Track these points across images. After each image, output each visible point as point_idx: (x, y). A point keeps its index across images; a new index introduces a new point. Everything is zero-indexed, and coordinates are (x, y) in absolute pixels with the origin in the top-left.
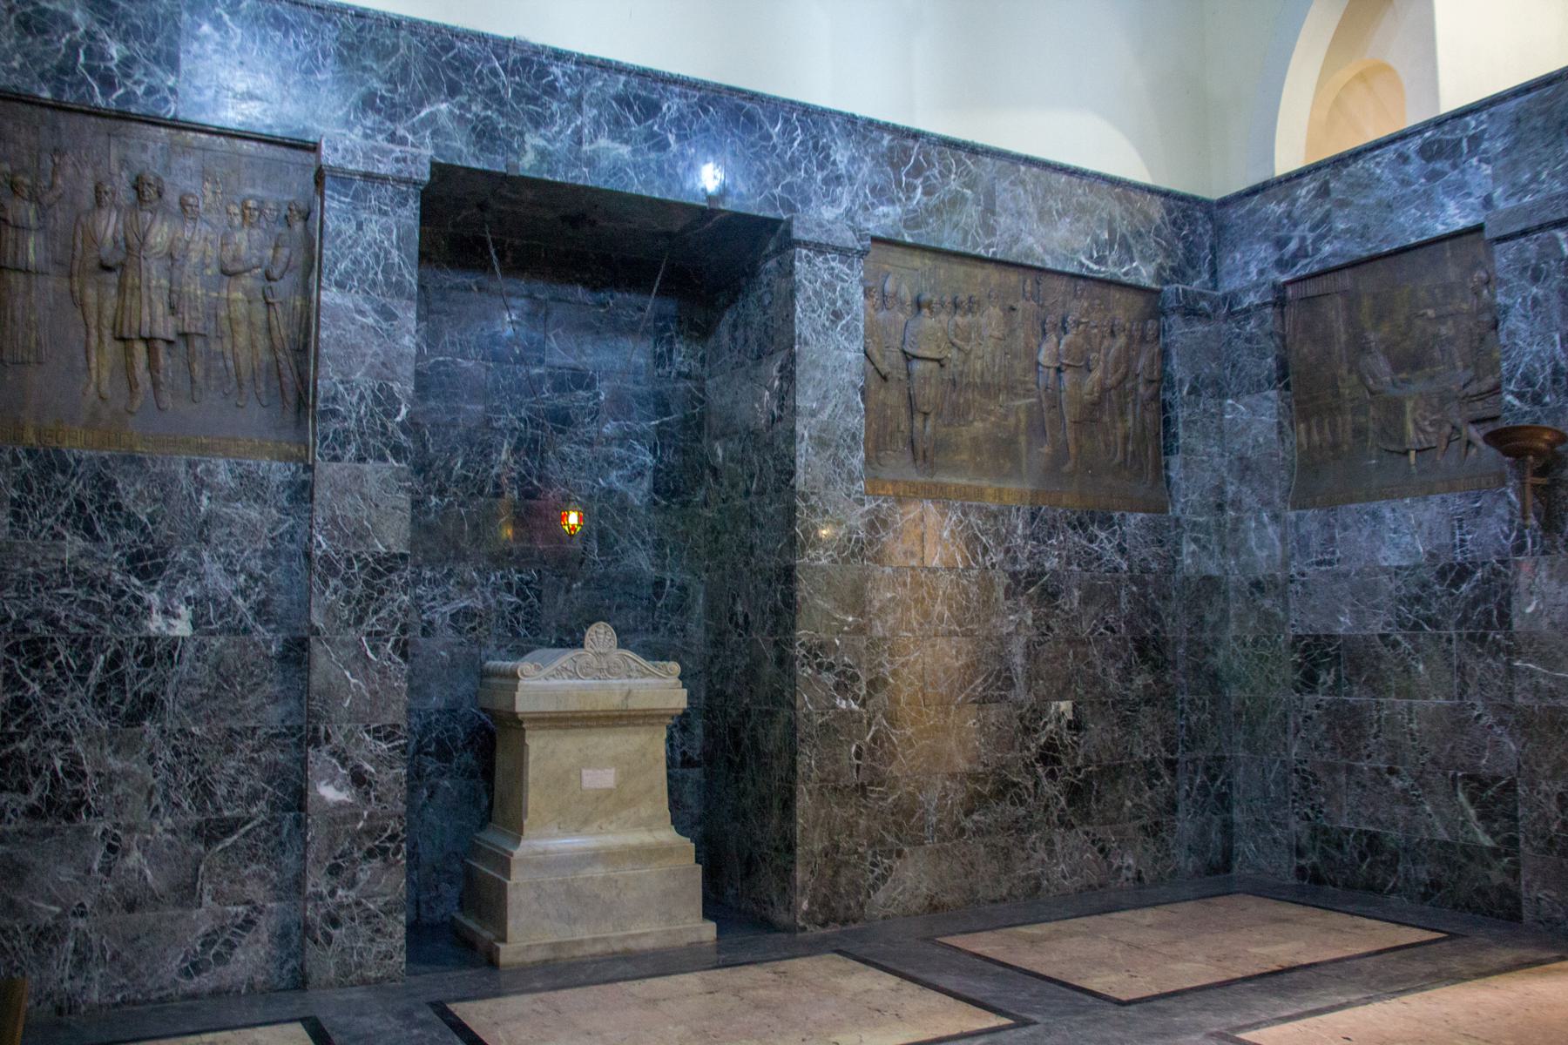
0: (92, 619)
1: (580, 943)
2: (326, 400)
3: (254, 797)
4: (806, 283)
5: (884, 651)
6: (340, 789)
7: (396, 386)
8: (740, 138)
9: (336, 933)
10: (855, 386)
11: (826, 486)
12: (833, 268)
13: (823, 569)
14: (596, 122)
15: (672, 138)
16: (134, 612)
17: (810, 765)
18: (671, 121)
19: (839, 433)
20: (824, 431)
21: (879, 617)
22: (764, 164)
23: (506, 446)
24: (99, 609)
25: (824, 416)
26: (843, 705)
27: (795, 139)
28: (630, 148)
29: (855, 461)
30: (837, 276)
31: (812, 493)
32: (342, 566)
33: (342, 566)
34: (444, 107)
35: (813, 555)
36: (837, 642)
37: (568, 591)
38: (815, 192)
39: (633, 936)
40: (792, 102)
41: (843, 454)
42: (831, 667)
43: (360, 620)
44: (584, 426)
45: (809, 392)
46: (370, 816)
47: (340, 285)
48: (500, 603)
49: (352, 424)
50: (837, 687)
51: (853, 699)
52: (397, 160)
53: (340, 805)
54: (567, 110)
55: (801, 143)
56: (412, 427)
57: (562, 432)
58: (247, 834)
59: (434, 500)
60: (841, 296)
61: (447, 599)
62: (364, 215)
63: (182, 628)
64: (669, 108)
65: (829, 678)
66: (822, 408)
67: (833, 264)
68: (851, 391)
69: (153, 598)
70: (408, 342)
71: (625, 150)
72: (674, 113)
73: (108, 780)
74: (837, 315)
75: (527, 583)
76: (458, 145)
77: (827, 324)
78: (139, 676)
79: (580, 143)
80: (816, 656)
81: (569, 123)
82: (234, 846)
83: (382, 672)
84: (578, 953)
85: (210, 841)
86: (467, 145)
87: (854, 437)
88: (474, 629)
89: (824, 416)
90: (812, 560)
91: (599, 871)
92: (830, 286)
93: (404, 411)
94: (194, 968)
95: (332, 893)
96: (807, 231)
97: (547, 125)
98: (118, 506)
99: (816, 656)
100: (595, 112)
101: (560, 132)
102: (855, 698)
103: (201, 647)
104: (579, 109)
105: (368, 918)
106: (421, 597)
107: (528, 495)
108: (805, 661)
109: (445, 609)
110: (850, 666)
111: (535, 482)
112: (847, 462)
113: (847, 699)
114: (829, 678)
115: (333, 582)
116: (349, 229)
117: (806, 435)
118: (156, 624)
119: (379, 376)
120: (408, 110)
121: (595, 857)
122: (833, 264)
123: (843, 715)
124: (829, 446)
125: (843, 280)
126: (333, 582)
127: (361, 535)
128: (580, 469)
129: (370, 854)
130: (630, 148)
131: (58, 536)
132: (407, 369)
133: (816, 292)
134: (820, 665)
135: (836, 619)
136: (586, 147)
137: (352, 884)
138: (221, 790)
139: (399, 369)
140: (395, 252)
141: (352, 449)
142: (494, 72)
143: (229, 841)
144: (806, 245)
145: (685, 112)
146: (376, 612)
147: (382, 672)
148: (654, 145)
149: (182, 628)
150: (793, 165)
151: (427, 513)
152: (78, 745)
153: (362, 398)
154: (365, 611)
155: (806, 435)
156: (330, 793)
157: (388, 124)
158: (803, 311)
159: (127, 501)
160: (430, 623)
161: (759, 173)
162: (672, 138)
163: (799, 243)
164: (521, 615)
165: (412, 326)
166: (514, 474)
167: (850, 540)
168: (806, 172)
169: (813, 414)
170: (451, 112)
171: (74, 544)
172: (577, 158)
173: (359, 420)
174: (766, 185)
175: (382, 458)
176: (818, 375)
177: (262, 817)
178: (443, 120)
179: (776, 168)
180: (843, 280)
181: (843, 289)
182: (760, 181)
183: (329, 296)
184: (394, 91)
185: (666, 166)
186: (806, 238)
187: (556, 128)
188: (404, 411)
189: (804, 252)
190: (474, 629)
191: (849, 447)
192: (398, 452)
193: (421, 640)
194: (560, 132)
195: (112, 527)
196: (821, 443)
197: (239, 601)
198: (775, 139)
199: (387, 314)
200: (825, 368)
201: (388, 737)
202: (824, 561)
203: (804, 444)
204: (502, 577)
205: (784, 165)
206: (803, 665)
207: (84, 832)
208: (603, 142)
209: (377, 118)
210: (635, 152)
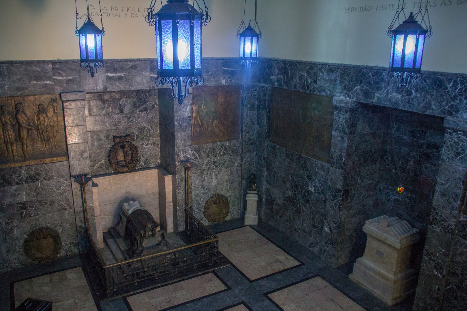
0: (303, 184)
1: (363, 285)
2: (332, 154)
3: (319, 224)
4: (448, 142)
5: (460, 266)
6: (328, 229)
7: (343, 154)
8: (436, 89)
9: (325, 254)
10: (460, 179)
11: (443, 208)
12: (460, 137)
13: (437, 232)
14: (393, 88)
15: (413, 91)
16: (308, 185)
17: (422, 282)
18: (414, 86)
19: (451, 193)
20: (446, 191)
21: (460, 255)
22: (443, 98)
23: (412, 161)
24: (303, 182)
25: (446, 186)
26: (436, 273)
27: (457, 88)
28: (401, 95)
29: (455, 204)
30: (461, 140)
31: (438, 209)
32: (332, 188)
33: (332, 188)
34: (359, 87)
35: (434, 227)
36: (438, 255)
37: (422, 203)
38: (462, 108)
39: (373, 291)
40: (456, 74)
41: (451, 200)
42: (434, 261)
43: (333, 200)
44: (434, 160)
45: (442, 178)
46: (331, 237)
47: (335, 131)
48: (405, 201)
49: (335, 160)
50: (435, 267)
51: (440, 273)
52: (345, 103)
53: (327, 232)
54: (386, 85)
55: (460, 89)
56: (344, 163)
57: (428, 160)
58: (318, 229)
59: (394, 171)
60: (461, 147)
61: (394, 195)
62: (340, 115)
63: (313, 190)
64: (414, 82)
65: (433, 264)
66: (446, 184)
67: (460, 136)
68: (458, 180)
69: (310, 184)
70: (345, 145)
71: (399, 96)
72: (415, 83)
73: (303, 211)
74: (458, 154)
75: (413, 198)
76: (361, 97)
77: (454, 156)
78: (308, 196)
79: (388, 95)
80: (430, 255)
81: (386, 89)
82: (316, 230)
83: (336, 211)
84: (362, 286)
85: (314, 228)
86: (363, 97)
87: (456, 196)
88: (398, 204)
89: (446, 186)
90: (433, 228)
91: (371, 273)
92: (457, 143)
93: (344, 160)
94: (310, 247)
95: (325, 247)
96: (449, 124)
97: (380, 90)
98: (306, 166)
99: (430, 255)
100: (393, 85)
101: (383, 92)
102: (441, 274)
103: (315, 195)
104: (389, 85)
105: (329, 254)
106: (388, 192)
107: (416, 175)
108: (426, 255)
109: (393, 197)
110: (441, 264)
111: (418, 172)
112: (452, 203)
113: (438, 272)
114: (433, 264)
115: (330, 191)
116: (337, 118)
117: (439, 190)
118: (310, 188)
119: (340, 151)
120: (352, 89)
121: (372, 270)
122: (460, 136)
123: (435, 275)
124: (446, 196)
125: (463, 142)
126: (330, 191)
127: (335, 184)
128: (431, 172)
129: (331, 244)
130: (401, 95)
131: (300, 169)
132: (345, 151)
133: (451, 145)
134: (430, 258)
135: (439, 249)
136: (389, 96)
137: (328, 247)
138: (315, 220)
139: (344, 151)
140: (345, 124)
141: (335, 166)
142: (370, 76)
143: (316, 229)
144: (449, 128)
145: (418, 82)
146: (336, 199)
147: (336, 211)
148: (408, 94)
149: (313, 190)
150: (455, 97)
151: (392, 173)
152: (300, 203)
153: (337, 155)
154: (334, 198)
155: (439, 190)
156: (326, 229)
157: (348, 92)
158: (445, 150)
159: (308, 166)
160: (389, 199)
161: (441, 101)
162: (413, 91)
163: (446, 128)
164: (409, 205)
165: (347, 141)
166: (413, 169)
167: (448, 227)
168: (460, 100)
169: (442, 185)
170: (360, 88)
171: (302, 171)
172: (387, 99)
173: (336, 160)
174: (443, 106)
175: (339, 169)
176: (447, 173)
177: (320, 228)
178: (358, 91)
179: (447, 99)
180: (463, 142)
181: (462, 145)
182: (440, 105)
183: (334, 133)
184: (349, 84)
185: (410, 100)
186: (448, 126)
187: (382, 91)
188: (344, 160)
189: (449, 130)
190: (398, 204)
191: (454, 199)
192: (342, 168)
193: (387, 203)
194: (383, 92)
195: (306, 170)
196: (443, 194)
197: (320, 188)
198: (449, 89)
199: (342, 138)
200: (449, 171)
201: (335, 224)
202: (437, 230)
203: (437, 193)
204: (407, 194)
205: (451, 98)
206: (425, 256)
207: (300, 217)
208: (394, 94)
209: (346, 91)
210: (402, 97)
